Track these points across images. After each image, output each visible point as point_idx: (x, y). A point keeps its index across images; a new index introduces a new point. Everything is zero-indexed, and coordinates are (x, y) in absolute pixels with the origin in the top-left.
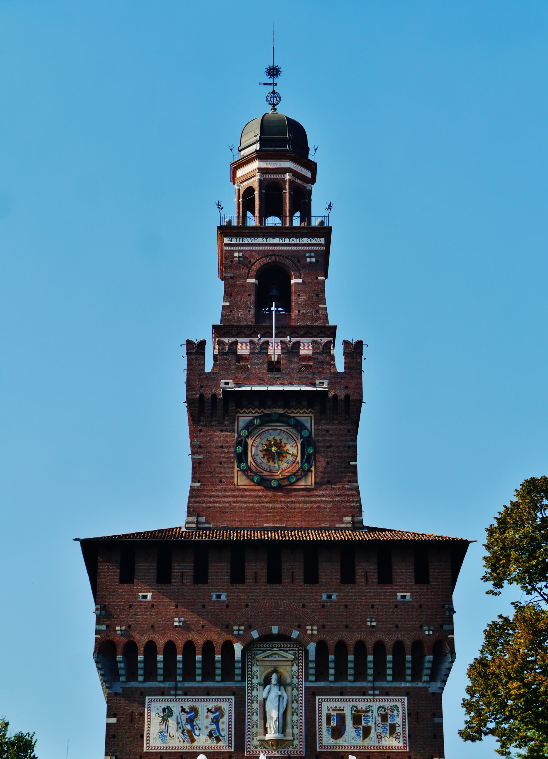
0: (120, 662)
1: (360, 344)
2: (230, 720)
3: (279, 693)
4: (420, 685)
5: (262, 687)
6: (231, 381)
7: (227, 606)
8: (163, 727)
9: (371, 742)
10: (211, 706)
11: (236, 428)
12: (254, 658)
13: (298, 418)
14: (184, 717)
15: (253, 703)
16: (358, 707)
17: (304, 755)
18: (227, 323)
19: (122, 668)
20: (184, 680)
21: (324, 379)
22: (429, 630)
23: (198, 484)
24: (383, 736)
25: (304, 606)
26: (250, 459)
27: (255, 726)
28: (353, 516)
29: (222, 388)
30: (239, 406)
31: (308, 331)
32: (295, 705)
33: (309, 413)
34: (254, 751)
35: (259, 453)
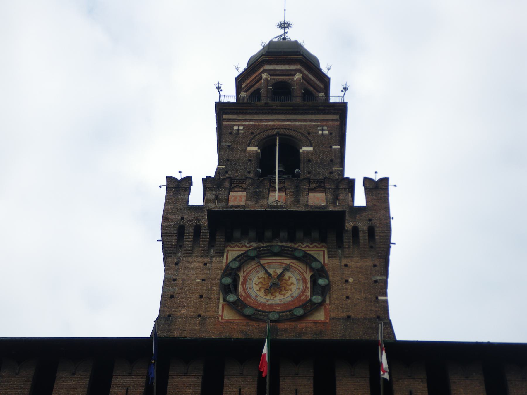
1: (385, 181)
11: (225, 261)
13: (307, 252)
30: (229, 239)
33: (321, 247)
35: (254, 285)
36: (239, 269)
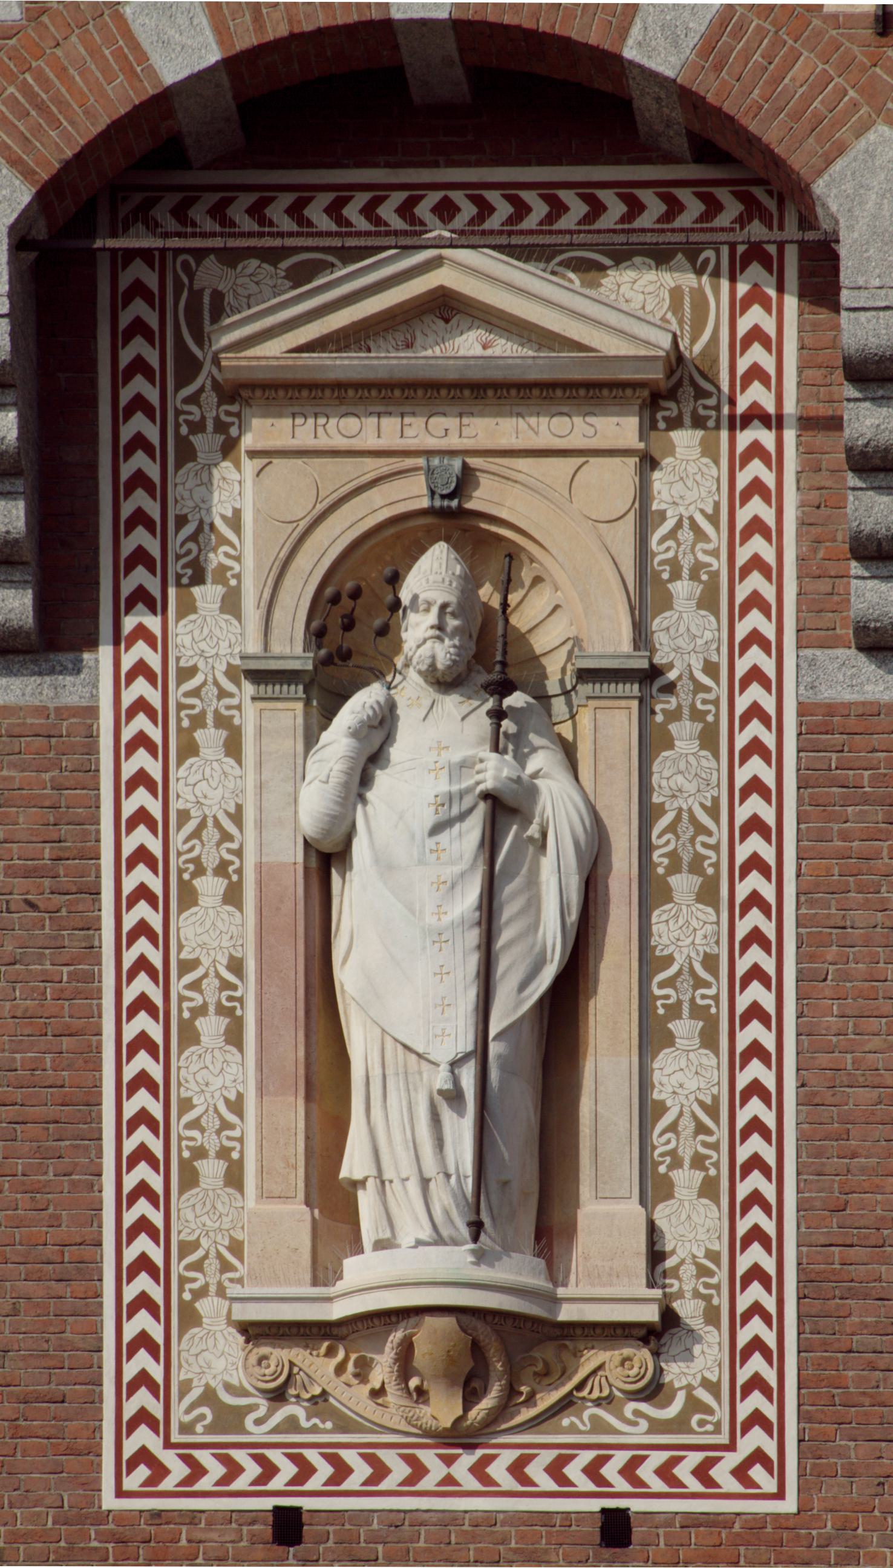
15: (189, 897)
17: (789, 1505)
27: (211, 1170)
34: (204, 1457)
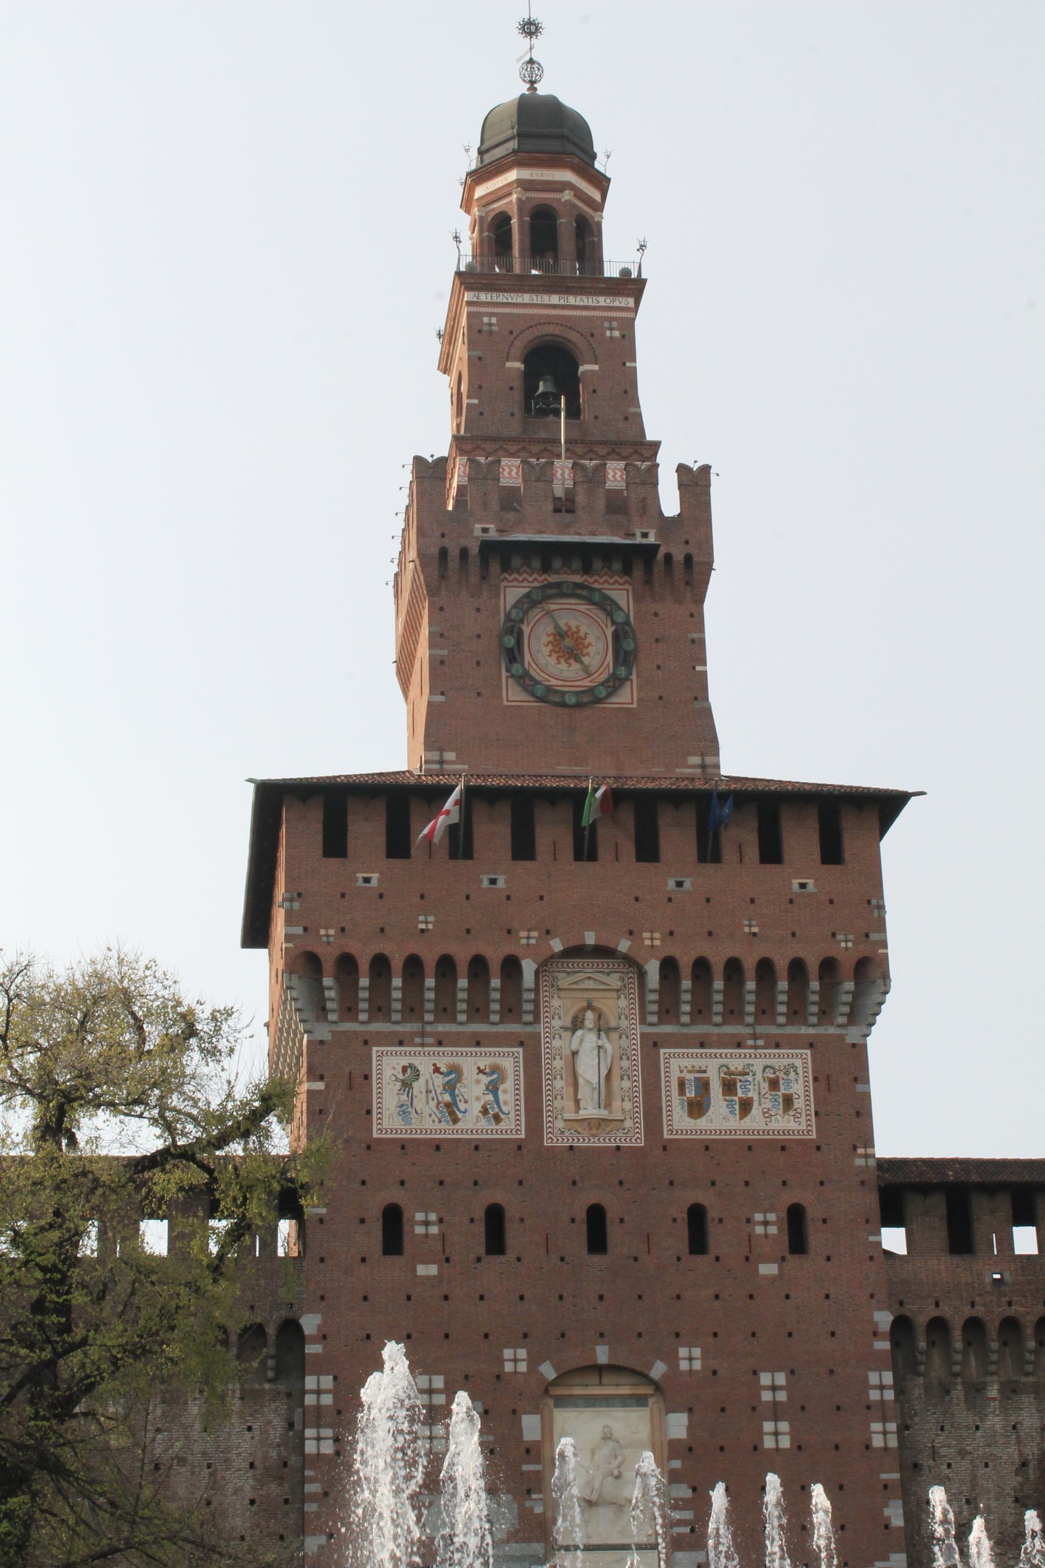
0: (329, 988)
1: (706, 469)
2: (517, 1086)
3: (600, 1043)
4: (832, 1030)
5: (569, 1033)
6: (492, 526)
7: (508, 898)
8: (404, 1097)
9: (754, 1124)
10: (484, 1063)
12: (553, 986)
13: (606, 592)
14: (439, 1080)
15: (555, 1059)
16: (730, 1066)
17: (643, 1145)
18: (475, 433)
19: (332, 1000)
20: (437, 1020)
21: (649, 527)
22: (846, 941)
23: (441, 698)
24: (772, 1113)
25: (637, 899)
26: (527, 658)
27: (559, 1097)
28: (702, 755)
29: (477, 538)
30: (506, 568)
31: (613, 451)
32: (625, 1064)
33: (623, 584)
35: (542, 646)
36: (522, 621)
